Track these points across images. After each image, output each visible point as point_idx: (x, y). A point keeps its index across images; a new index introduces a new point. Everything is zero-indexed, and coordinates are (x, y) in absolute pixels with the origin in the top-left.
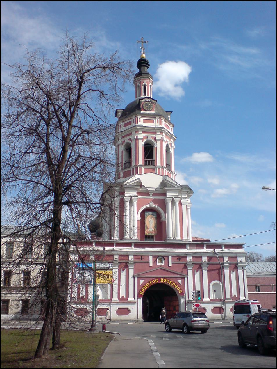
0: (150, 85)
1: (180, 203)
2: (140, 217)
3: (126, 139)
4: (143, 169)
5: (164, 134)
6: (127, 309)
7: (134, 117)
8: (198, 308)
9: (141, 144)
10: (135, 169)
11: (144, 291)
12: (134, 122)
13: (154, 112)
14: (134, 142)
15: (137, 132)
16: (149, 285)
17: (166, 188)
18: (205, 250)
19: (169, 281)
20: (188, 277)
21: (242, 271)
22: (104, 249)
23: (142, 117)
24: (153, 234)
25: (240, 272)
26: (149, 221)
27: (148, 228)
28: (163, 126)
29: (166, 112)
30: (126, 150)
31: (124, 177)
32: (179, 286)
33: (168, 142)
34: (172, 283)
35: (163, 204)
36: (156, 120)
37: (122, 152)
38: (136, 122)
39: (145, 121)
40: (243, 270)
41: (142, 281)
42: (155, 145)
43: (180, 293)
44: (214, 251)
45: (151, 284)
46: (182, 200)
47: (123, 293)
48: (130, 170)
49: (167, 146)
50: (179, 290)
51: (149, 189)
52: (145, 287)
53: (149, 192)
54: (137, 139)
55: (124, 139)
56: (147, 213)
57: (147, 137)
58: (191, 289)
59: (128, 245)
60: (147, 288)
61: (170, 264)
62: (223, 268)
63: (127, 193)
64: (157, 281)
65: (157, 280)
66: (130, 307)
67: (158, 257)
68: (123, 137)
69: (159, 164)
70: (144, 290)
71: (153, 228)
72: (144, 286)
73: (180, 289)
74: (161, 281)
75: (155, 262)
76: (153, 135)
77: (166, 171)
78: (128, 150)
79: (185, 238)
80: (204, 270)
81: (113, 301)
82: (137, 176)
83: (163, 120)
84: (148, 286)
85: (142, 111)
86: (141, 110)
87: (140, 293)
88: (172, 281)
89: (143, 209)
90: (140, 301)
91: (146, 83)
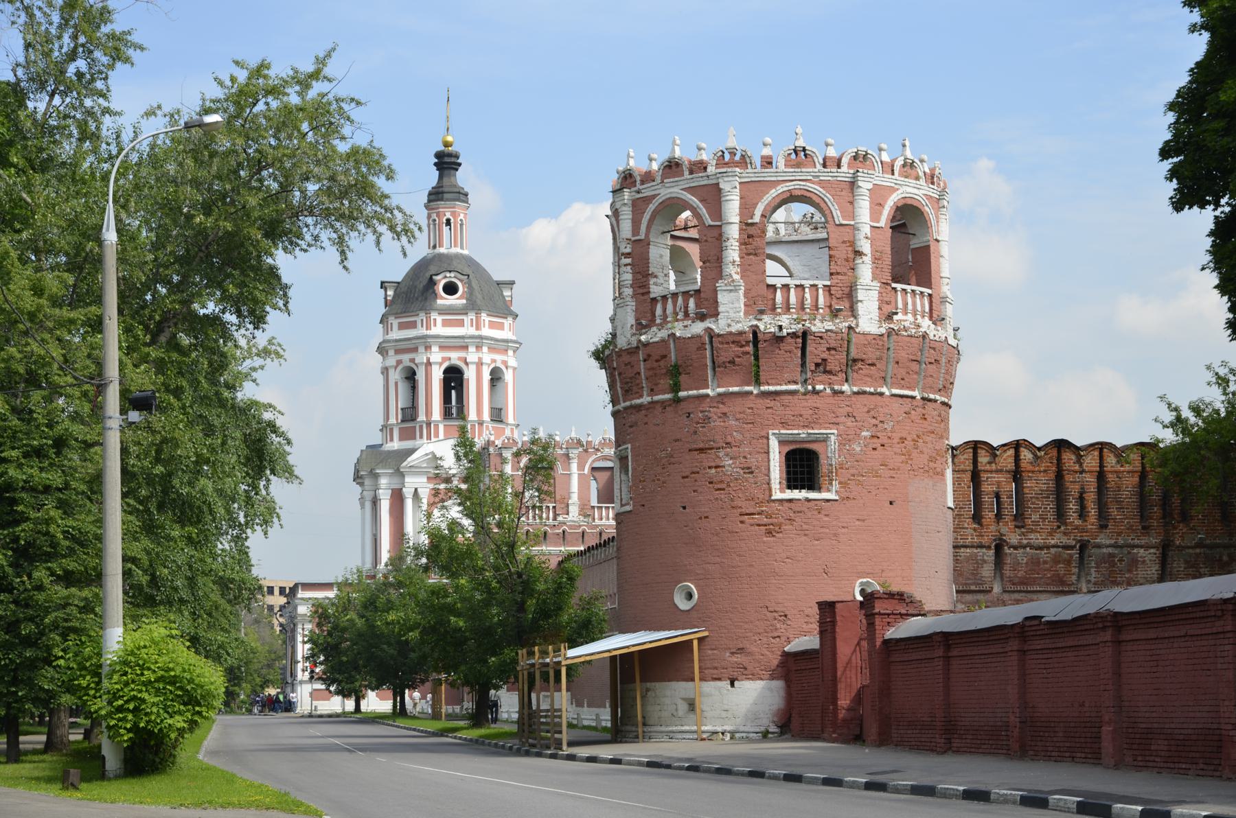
0: (461, 220)
3: (406, 358)
4: (441, 427)
5: (485, 349)
7: (422, 315)
9: (438, 374)
10: (425, 426)
12: (422, 326)
15: (428, 348)
28: (486, 331)
30: (406, 378)
33: (494, 361)
36: (467, 319)
38: (428, 328)
39: (446, 323)
54: (429, 364)
76: (462, 354)
83: (482, 318)
91: (451, 218)
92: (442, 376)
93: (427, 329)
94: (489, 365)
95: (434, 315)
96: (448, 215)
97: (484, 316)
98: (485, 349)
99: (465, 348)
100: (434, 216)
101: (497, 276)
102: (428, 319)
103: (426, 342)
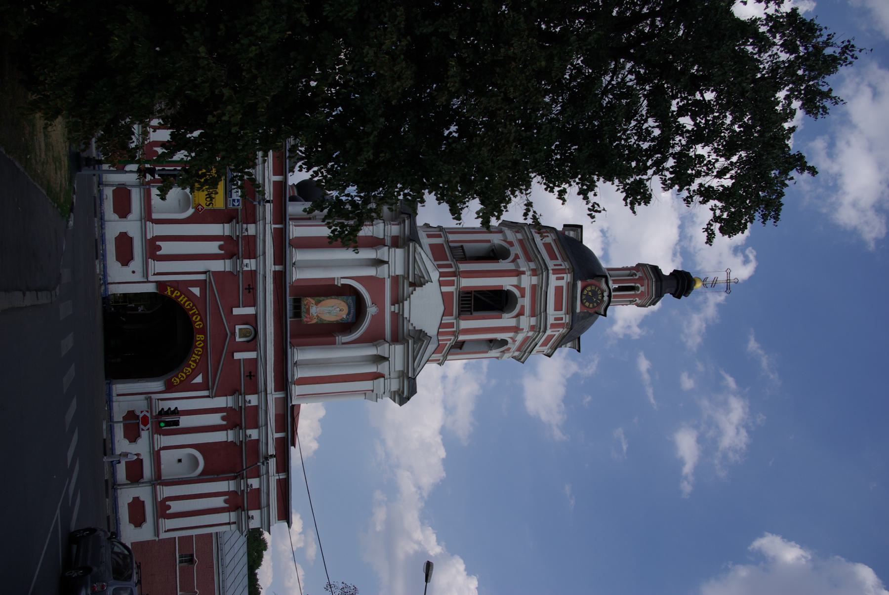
0: (636, 300)
1: (377, 376)
2: (342, 284)
3: (516, 250)
5: (531, 334)
6: (132, 258)
7: (565, 265)
8: (138, 423)
9: (507, 283)
11: (173, 296)
12: (555, 265)
13: (578, 310)
14: (512, 266)
15: (534, 272)
16: (189, 307)
17: (410, 341)
18: (274, 435)
19: (199, 353)
20: (208, 397)
21: (228, 521)
22: (268, 202)
23: (568, 284)
24: (305, 318)
25: (224, 517)
26: (333, 307)
27: (317, 303)
29: (579, 339)
30: (493, 250)
31: (432, 246)
32: (188, 376)
34: (194, 361)
35: (373, 338)
37: (489, 241)
38: (555, 271)
39: (559, 290)
40: (229, 524)
41: (196, 291)
42: (505, 315)
43: (173, 380)
44: (271, 456)
45: (191, 313)
46: (383, 379)
47: (167, 248)
48: (448, 260)
49: (504, 342)
50: (180, 376)
51: (406, 303)
52: (184, 298)
53: (401, 304)
55: (516, 244)
56: (350, 300)
57: (523, 296)
58: (182, 405)
59: (281, 257)
60: (182, 302)
61: (238, 356)
62: (234, 478)
63: (399, 253)
64: (198, 327)
65: (201, 326)
66: (137, 263)
67: (254, 328)
68: (521, 242)
69: (465, 324)
70: (176, 296)
71: (317, 316)
72: (186, 296)
73: (182, 379)
74: (198, 336)
75: (244, 319)
77: (449, 342)
78: (492, 254)
79: (297, 390)
80: (227, 433)
81: (149, 224)
82: (435, 275)
84: (186, 305)
85: (579, 284)
86: (581, 280)
87: (169, 288)
88: (199, 360)
89: (360, 290)
90: (150, 288)
91: (640, 292)
92: (505, 289)
93: (553, 270)
94: (511, 338)
95: (568, 277)
96: (642, 289)
97: (562, 331)
98: (531, 334)
99: (533, 314)
100: (639, 274)
101: (582, 337)
102: (562, 271)
103: (540, 270)
